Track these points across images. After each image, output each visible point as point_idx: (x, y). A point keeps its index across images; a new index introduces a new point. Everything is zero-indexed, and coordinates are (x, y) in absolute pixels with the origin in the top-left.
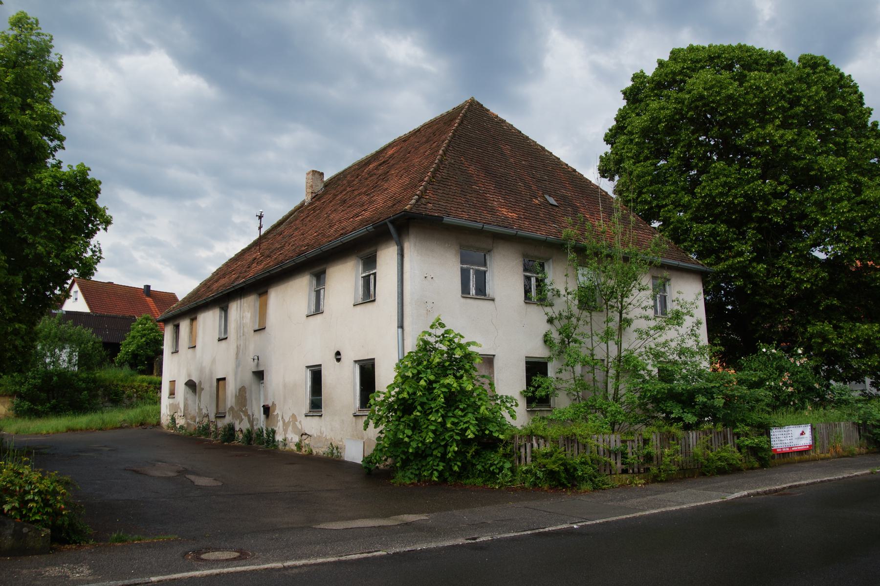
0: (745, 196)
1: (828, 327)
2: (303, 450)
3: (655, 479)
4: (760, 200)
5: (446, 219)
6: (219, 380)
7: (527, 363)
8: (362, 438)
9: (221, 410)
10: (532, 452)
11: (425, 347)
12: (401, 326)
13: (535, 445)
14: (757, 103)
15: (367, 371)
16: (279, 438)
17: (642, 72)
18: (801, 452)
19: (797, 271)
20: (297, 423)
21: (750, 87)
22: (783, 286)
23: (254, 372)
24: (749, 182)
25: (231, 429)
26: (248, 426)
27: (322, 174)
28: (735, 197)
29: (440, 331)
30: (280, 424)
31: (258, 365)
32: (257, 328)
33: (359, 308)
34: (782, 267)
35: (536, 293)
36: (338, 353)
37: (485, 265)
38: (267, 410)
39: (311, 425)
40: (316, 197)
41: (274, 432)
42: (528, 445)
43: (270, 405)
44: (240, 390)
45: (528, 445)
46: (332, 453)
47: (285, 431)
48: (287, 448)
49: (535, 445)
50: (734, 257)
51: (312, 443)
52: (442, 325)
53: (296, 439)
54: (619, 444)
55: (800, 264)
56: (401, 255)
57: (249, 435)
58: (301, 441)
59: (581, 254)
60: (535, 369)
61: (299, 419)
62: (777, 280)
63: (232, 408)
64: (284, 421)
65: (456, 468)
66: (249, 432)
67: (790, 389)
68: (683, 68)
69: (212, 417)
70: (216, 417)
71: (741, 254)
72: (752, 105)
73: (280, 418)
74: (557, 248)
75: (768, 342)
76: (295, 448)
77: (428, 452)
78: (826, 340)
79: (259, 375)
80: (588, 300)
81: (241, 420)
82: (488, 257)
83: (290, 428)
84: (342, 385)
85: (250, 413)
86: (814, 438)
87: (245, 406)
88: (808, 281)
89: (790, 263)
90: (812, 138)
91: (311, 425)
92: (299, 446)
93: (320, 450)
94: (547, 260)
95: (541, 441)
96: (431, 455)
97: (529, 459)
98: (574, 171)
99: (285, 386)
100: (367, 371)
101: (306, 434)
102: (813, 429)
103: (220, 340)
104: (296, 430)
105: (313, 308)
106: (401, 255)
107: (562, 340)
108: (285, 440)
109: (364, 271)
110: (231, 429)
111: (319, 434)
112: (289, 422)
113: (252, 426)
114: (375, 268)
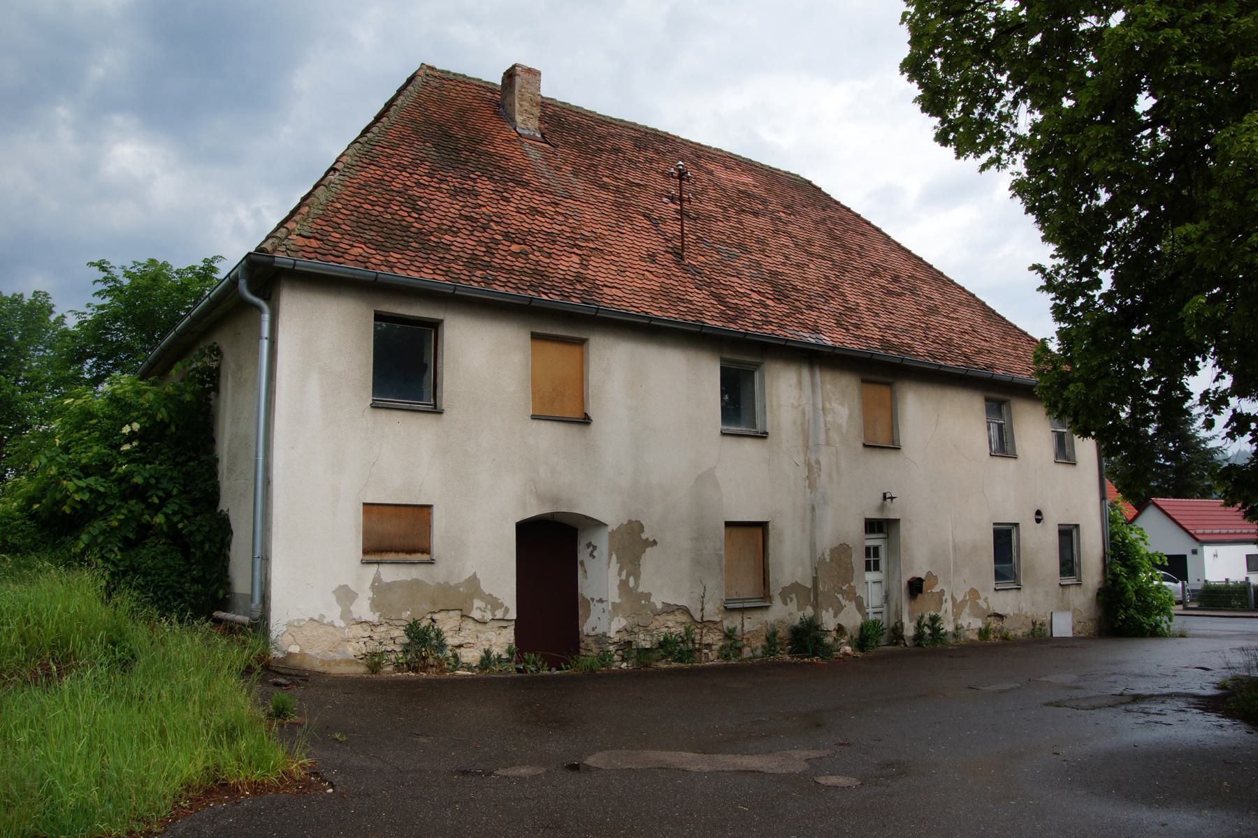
6: (729, 524)
15: (1068, 534)
16: (948, 627)
20: (981, 602)
30: (948, 605)
31: (882, 508)
39: (1004, 602)
41: (934, 619)
44: (833, 551)
47: (957, 615)
51: (1006, 624)
53: (978, 624)
57: (865, 638)
61: (983, 595)
63: (795, 588)
73: (947, 596)
76: (975, 637)
81: (839, 609)
83: (967, 610)
92: (984, 633)
93: (1019, 630)
100: (1068, 534)
104: (977, 612)
111: (1017, 612)
112: (964, 601)
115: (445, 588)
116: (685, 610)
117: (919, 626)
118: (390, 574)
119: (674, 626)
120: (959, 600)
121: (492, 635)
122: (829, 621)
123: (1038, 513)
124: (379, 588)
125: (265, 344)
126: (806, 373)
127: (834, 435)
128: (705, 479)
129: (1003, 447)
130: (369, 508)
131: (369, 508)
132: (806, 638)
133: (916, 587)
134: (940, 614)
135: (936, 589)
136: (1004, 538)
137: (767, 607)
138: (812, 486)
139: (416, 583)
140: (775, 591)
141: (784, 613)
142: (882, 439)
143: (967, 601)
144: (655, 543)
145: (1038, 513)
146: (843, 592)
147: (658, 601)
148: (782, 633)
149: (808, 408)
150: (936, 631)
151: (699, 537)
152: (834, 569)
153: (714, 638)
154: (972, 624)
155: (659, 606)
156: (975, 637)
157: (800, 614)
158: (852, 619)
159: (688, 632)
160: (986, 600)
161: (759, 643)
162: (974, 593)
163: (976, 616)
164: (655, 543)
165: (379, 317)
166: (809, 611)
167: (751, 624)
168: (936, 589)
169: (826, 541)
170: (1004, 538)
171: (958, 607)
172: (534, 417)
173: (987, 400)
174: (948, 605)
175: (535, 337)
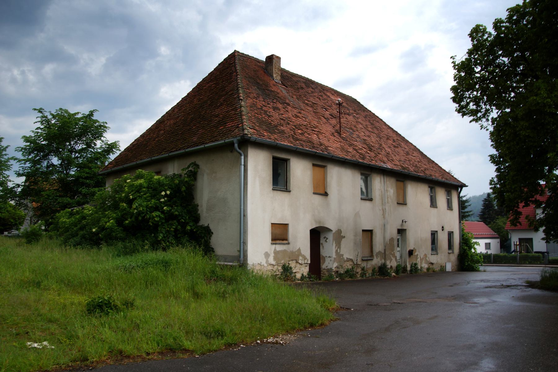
6: (363, 231)
15: (450, 234)
20: (427, 258)
30: (419, 260)
31: (402, 225)
39: (433, 259)
41: (416, 264)
47: (421, 263)
51: (434, 266)
61: (428, 256)
63: (379, 252)
73: (419, 256)
76: (426, 271)
79: (401, 232)
81: (391, 260)
83: (424, 261)
92: (428, 269)
100: (450, 234)
104: (427, 262)
115: (292, 253)
116: (351, 260)
117: (411, 266)
118: (279, 248)
119: (348, 266)
121: (303, 269)
122: (389, 264)
123: (443, 227)
124: (276, 252)
125: (243, 167)
127: (390, 200)
128: (357, 215)
129: (433, 204)
130: (273, 224)
131: (273, 224)
132: (382, 270)
133: (411, 253)
135: (416, 254)
137: (372, 260)
138: (384, 217)
139: (285, 251)
140: (374, 254)
141: (377, 262)
142: (401, 202)
143: (425, 258)
144: (344, 237)
145: (443, 227)
146: (392, 254)
147: (346, 256)
149: (383, 190)
150: (416, 269)
151: (356, 235)
152: (389, 246)
153: (359, 270)
155: (345, 259)
157: (381, 262)
159: (353, 268)
161: (370, 272)
162: (425, 255)
164: (344, 237)
165: (274, 158)
166: (383, 261)
168: (416, 254)
169: (388, 237)
171: (421, 260)
172: (314, 193)
175: (314, 165)
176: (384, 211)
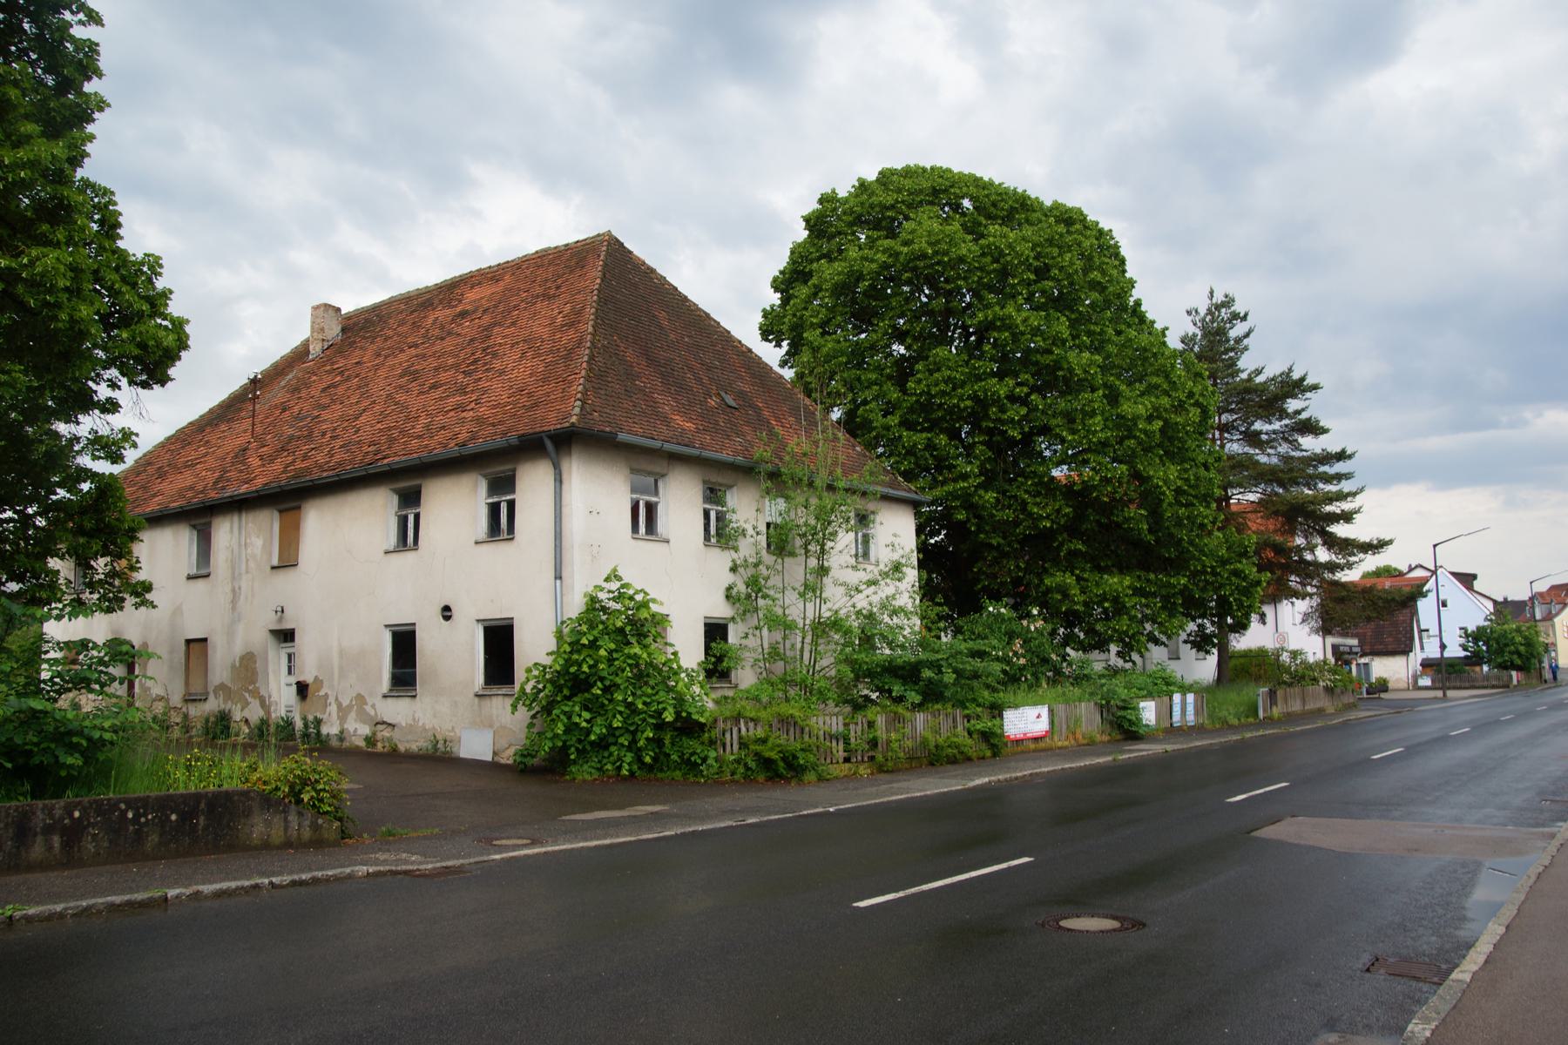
0: (974, 398)
1: (1071, 580)
2: (380, 745)
3: (881, 769)
4: (993, 404)
5: (622, 437)
6: (188, 642)
7: (706, 625)
8: (491, 726)
9: (196, 688)
10: (740, 738)
11: (593, 604)
12: (558, 576)
13: (743, 729)
14: (995, 270)
17: (833, 191)
18: (1036, 739)
19: (1037, 504)
20: (368, 708)
21: (989, 246)
22: (1016, 523)
23: (273, 632)
24: (979, 378)
25: (224, 718)
26: (261, 713)
27: (339, 310)
28: (961, 399)
29: (614, 586)
31: (280, 620)
32: (275, 562)
33: (485, 547)
34: (1015, 497)
35: (719, 533)
36: (447, 609)
37: (656, 493)
38: (302, 689)
39: (398, 711)
40: (333, 350)
41: (318, 722)
42: (735, 731)
43: (308, 678)
44: (242, 658)
45: (735, 731)
46: (436, 750)
47: (342, 719)
48: (346, 744)
49: (743, 729)
50: (955, 480)
51: (396, 735)
52: (619, 578)
53: (365, 730)
54: (841, 728)
55: (1038, 494)
56: (559, 480)
57: (262, 729)
58: (374, 734)
59: (776, 481)
60: (715, 632)
61: (370, 701)
62: (1008, 515)
63: (222, 687)
64: (339, 706)
65: (648, 759)
66: (264, 722)
67: (1022, 661)
68: (897, 201)
69: (176, 699)
70: (186, 701)
71: (965, 477)
72: (989, 273)
73: (331, 699)
74: (746, 471)
75: (996, 597)
76: (362, 744)
77: (611, 740)
78: (1066, 595)
79: (286, 636)
80: (779, 541)
82: (660, 484)
83: (353, 715)
84: (455, 655)
85: (263, 692)
86: (1052, 722)
87: (254, 682)
88: (1048, 517)
89: (1026, 492)
90: (1062, 327)
91: (398, 711)
92: (371, 741)
93: (414, 744)
94: (730, 487)
95: (751, 725)
96: (615, 744)
97: (736, 746)
98: (750, 351)
99: (341, 653)
101: (384, 723)
102: (1051, 711)
103: (190, 578)
104: (363, 717)
105: (392, 539)
106: (559, 480)
107: (749, 595)
108: (342, 732)
109: (490, 494)
110: (224, 718)
111: (410, 722)
112: (350, 707)
113: (268, 713)
114: (513, 491)
117: (306, 726)
119: (159, 708)
120: (345, 703)
126: (236, 518)
127: (252, 565)
134: (325, 717)
135: (322, 693)
136: (404, 643)
138: (234, 608)
140: (211, 689)
141: (212, 705)
143: (359, 704)
145: (447, 609)
148: (212, 719)
149: (236, 548)
150: (319, 733)
151: (171, 652)
152: (248, 668)
154: (358, 730)
156: (362, 744)
158: (255, 713)
160: (373, 706)
162: (360, 699)
163: (364, 722)
167: (194, 711)
168: (322, 693)
170: (404, 643)
171: (343, 712)
173: (395, 491)
174: (333, 708)
176: (235, 593)
